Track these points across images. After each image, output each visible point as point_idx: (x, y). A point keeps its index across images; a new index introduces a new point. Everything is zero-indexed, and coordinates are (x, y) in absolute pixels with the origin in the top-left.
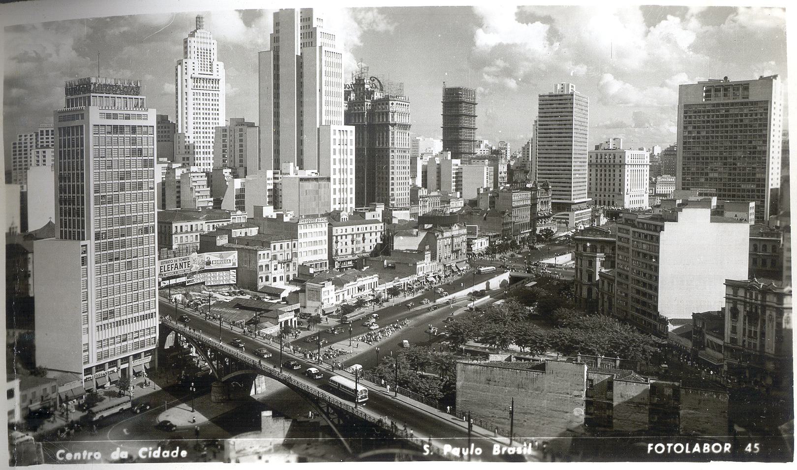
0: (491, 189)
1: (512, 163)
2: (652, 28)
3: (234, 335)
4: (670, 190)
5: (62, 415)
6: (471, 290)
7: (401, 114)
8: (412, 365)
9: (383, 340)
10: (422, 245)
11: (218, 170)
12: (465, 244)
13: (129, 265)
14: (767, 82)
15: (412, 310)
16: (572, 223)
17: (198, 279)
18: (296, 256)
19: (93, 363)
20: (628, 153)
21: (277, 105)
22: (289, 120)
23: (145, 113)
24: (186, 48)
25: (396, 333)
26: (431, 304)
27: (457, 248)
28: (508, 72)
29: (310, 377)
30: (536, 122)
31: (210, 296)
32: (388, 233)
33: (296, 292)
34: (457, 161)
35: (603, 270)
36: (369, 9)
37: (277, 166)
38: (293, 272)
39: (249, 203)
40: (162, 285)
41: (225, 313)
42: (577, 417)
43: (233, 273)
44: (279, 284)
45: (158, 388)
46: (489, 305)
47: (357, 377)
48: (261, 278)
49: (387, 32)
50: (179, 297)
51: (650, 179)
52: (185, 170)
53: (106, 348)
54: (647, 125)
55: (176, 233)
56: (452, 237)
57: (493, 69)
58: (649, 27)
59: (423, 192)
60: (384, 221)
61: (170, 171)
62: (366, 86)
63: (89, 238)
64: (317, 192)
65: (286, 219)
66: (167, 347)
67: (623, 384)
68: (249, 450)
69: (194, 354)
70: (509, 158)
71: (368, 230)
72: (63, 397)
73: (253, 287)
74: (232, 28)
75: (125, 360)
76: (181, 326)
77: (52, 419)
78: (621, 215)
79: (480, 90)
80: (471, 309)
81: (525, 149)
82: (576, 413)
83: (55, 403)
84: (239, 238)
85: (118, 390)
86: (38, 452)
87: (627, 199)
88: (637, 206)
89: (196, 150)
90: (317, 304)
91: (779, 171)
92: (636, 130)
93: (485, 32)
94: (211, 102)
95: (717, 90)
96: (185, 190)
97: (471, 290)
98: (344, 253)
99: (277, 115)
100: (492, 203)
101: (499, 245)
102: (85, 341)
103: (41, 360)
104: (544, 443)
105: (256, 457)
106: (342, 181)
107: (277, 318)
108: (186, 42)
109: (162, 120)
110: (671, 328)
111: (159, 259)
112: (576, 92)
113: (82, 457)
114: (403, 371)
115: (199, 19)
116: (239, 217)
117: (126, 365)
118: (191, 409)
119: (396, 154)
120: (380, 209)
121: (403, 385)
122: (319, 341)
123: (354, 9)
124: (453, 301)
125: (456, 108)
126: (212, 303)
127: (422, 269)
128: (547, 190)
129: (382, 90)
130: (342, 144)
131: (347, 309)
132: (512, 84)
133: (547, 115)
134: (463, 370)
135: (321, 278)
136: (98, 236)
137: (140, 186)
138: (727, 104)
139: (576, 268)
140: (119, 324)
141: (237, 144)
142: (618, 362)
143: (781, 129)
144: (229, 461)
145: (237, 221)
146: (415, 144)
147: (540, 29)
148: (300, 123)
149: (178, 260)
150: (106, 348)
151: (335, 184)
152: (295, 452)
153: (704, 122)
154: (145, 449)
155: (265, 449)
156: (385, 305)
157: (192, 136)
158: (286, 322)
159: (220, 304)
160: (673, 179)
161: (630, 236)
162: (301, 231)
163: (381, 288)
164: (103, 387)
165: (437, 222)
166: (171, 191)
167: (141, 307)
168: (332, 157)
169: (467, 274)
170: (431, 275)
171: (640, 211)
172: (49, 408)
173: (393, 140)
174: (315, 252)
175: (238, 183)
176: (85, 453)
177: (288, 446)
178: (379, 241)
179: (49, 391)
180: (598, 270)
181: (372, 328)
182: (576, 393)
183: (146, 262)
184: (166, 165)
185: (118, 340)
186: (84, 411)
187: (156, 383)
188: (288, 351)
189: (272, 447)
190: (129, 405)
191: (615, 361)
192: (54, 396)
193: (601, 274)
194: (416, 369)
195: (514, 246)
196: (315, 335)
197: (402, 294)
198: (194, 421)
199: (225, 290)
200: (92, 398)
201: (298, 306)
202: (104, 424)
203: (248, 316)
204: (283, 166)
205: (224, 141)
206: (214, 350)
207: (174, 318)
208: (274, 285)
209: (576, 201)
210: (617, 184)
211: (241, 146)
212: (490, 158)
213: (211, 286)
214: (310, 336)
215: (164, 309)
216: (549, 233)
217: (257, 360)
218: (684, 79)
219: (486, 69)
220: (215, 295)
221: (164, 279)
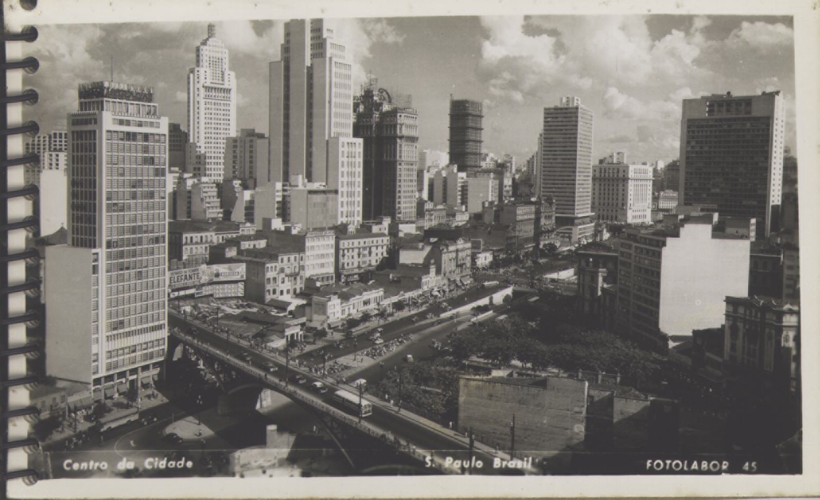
0: (496, 203)
1: (517, 177)
2: (657, 43)
3: (242, 348)
4: (672, 205)
5: (70, 426)
6: (474, 304)
7: (409, 126)
8: (415, 381)
9: (388, 355)
10: (428, 259)
11: (228, 181)
12: (469, 258)
13: (139, 275)
14: (769, 98)
15: (417, 325)
16: (575, 238)
17: (207, 291)
19: (103, 373)
20: (632, 168)
21: (287, 117)
22: (299, 132)
23: (157, 121)
24: (198, 56)
25: (401, 348)
26: (435, 319)
27: (462, 262)
28: (514, 85)
29: (315, 391)
30: (541, 135)
31: (218, 308)
32: (394, 247)
33: (303, 306)
34: (463, 175)
35: (605, 286)
36: (378, 20)
37: (286, 178)
38: (300, 285)
39: (258, 216)
40: (172, 296)
41: (233, 326)
42: (577, 434)
43: (241, 286)
44: (286, 298)
45: (166, 400)
46: (492, 320)
47: (361, 391)
48: (269, 291)
49: (396, 44)
50: (188, 309)
51: (653, 194)
52: (196, 180)
53: (115, 359)
54: (650, 139)
55: (186, 244)
56: (457, 251)
57: (499, 82)
58: (654, 41)
59: (429, 206)
60: (390, 234)
61: (181, 181)
62: (375, 98)
63: (101, 246)
64: (325, 205)
65: (294, 232)
66: (175, 359)
67: (623, 401)
68: (254, 464)
69: (201, 366)
70: (514, 171)
71: (375, 243)
72: (72, 407)
73: (260, 299)
74: (244, 39)
75: (134, 371)
76: (189, 338)
77: (60, 429)
78: (624, 230)
79: (486, 102)
80: (474, 324)
81: (530, 163)
82: (576, 430)
83: (64, 413)
84: (248, 251)
85: (125, 401)
86: (46, 462)
87: (630, 214)
88: (639, 221)
89: (207, 161)
90: (322, 318)
91: (780, 188)
92: (640, 144)
93: (493, 44)
94: (222, 112)
95: (720, 105)
96: (195, 200)
97: (474, 304)
99: (287, 126)
100: (497, 216)
101: (503, 259)
102: (94, 351)
103: (52, 370)
104: (544, 459)
105: (260, 471)
106: (351, 194)
107: (283, 331)
108: (198, 50)
109: (174, 129)
110: (671, 344)
111: (170, 269)
112: (581, 106)
113: (89, 466)
114: (406, 385)
115: (211, 28)
116: (249, 229)
117: (135, 377)
118: (197, 422)
119: (404, 167)
120: (387, 222)
121: (405, 400)
122: (324, 355)
123: (363, 21)
124: (457, 315)
125: (463, 120)
126: (220, 315)
127: (426, 283)
128: (551, 204)
129: (390, 102)
131: (352, 323)
132: (518, 96)
133: (553, 128)
134: (466, 386)
135: (327, 292)
136: (109, 245)
137: (151, 195)
138: (730, 120)
139: (579, 284)
140: (128, 334)
141: (248, 155)
142: (618, 379)
143: (783, 145)
144: (233, 475)
145: (246, 233)
146: (422, 157)
147: (546, 42)
148: (310, 135)
149: (187, 271)
150: (115, 359)
151: (342, 196)
152: (299, 467)
153: (706, 137)
154: (151, 460)
155: (269, 464)
156: (390, 319)
157: (203, 146)
158: (292, 336)
159: (228, 317)
160: (675, 195)
161: (632, 252)
162: (308, 244)
163: (386, 302)
164: (111, 398)
165: (444, 235)
166: (181, 199)
167: (150, 318)
168: (341, 169)
169: (471, 288)
170: (436, 289)
171: (643, 226)
172: (58, 418)
174: (322, 265)
175: (247, 195)
176: (92, 463)
177: (292, 460)
178: (385, 255)
179: (58, 400)
180: (600, 285)
181: (377, 342)
182: (577, 409)
183: (156, 273)
184: (177, 175)
185: (126, 351)
186: (92, 421)
187: (164, 395)
188: (293, 364)
189: (276, 461)
190: (136, 417)
191: (615, 378)
192: (63, 405)
193: (603, 289)
194: (420, 385)
195: (517, 261)
196: (321, 349)
197: (407, 309)
198: (200, 434)
199: (233, 302)
200: (100, 410)
201: (303, 320)
202: (113, 435)
203: (255, 329)
204: (292, 178)
205: (234, 152)
206: (222, 362)
207: (182, 330)
208: (281, 298)
209: (580, 215)
210: (620, 198)
211: (251, 157)
212: (495, 172)
213: (220, 299)
214: (316, 350)
215: (174, 321)
216: (552, 247)
217: (263, 374)
218: (688, 93)
219: (493, 81)
220: (224, 307)
221: (173, 291)
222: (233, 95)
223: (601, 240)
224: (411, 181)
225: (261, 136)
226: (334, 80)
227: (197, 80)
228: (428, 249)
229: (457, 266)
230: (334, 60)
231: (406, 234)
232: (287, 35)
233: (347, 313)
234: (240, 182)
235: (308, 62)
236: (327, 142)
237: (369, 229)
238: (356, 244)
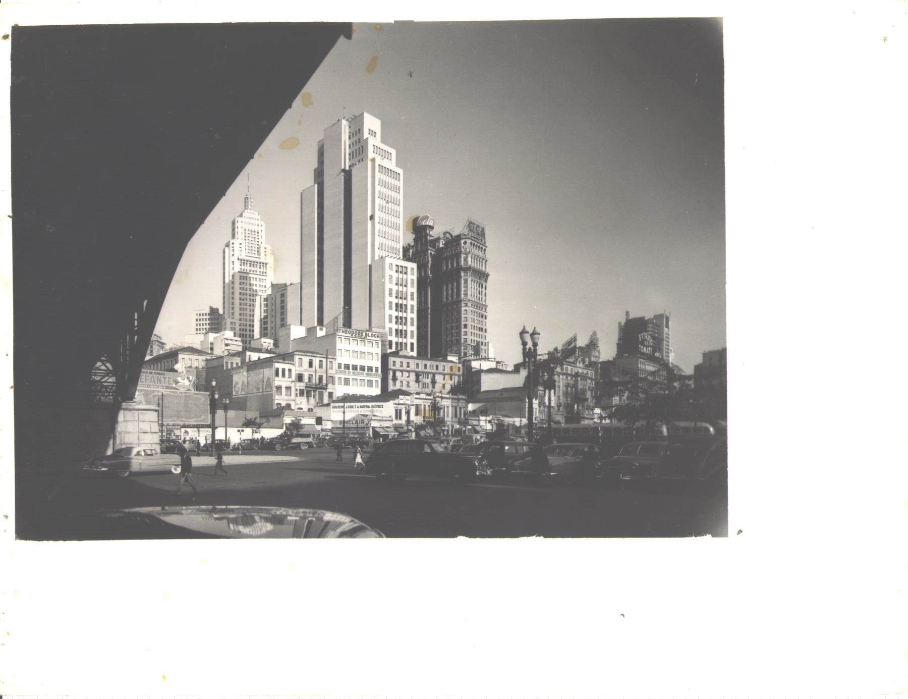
18: (333, 384)
71: (441, 369)
130: (397, 282)
226: (378, 240)
236: (370, 266)
238: (413, 366)
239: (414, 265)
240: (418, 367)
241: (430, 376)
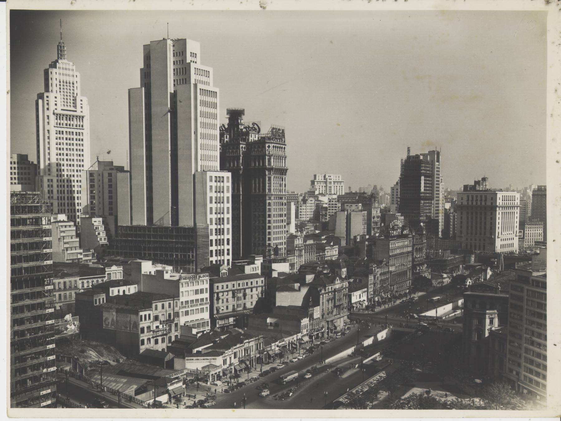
18: (178, 316)
71: (249, 285)
87: (498, 243)
98: (225, 311)
120: (259, 261)
173: (270, 186)
222: (86, 123)
223: (485, 279)
224: (281, 215)
225: (121, 169)
227: (46, 106)
228: (304, 291)
229: (335, 306)
230: (200, 86)
231: (280, 274)
232: (147, 58)
233: (228, 362)
234: (101, 219)
235: (171, 89)
237: (242, 269)
238: (230, 287)
239: (229, 174)
240: (234, 287)
241: (242, 291)
